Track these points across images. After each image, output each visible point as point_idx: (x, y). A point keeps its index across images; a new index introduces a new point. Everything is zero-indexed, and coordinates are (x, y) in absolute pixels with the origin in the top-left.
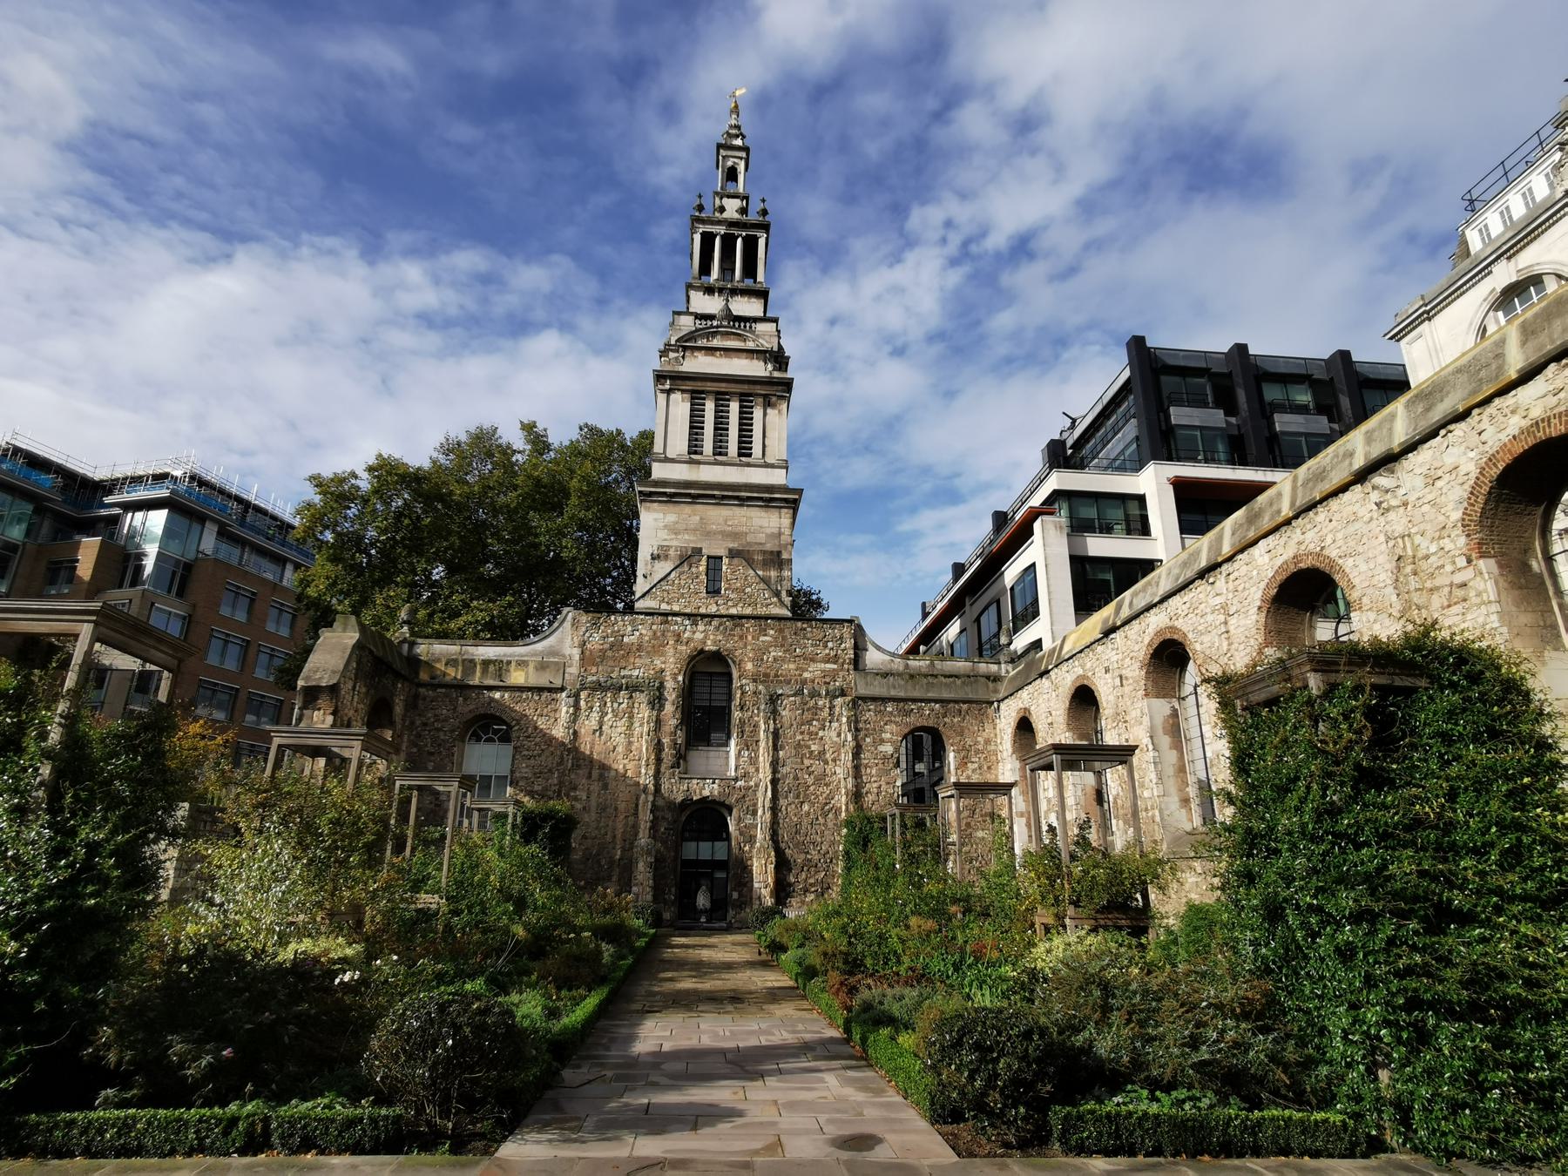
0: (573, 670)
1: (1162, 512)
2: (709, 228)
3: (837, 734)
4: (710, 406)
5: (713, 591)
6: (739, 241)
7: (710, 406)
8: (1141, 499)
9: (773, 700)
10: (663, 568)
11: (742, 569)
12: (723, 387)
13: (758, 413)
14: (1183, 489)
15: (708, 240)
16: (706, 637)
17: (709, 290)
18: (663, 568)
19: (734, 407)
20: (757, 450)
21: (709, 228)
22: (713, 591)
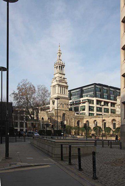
0: (54, 115)
1: (95, 102)
2: (60, 65)
3: (73, 121)
4: (62, 88)
5: (63, 107)
6: (62, 68)
7: (62, 88)
8: (93, 100)
9: (69, 118)
10: (59, 105)
11: (65, 106)
12: (63, 86)
13: (66, 89)
14: (97, 101)
15: (59, 66)
16: (64, 112)
17: (60, 73)
18: (59, 105)
19: (64, 88)
20: (66, 93)
21: (60, 65)
22: (63, 107)
